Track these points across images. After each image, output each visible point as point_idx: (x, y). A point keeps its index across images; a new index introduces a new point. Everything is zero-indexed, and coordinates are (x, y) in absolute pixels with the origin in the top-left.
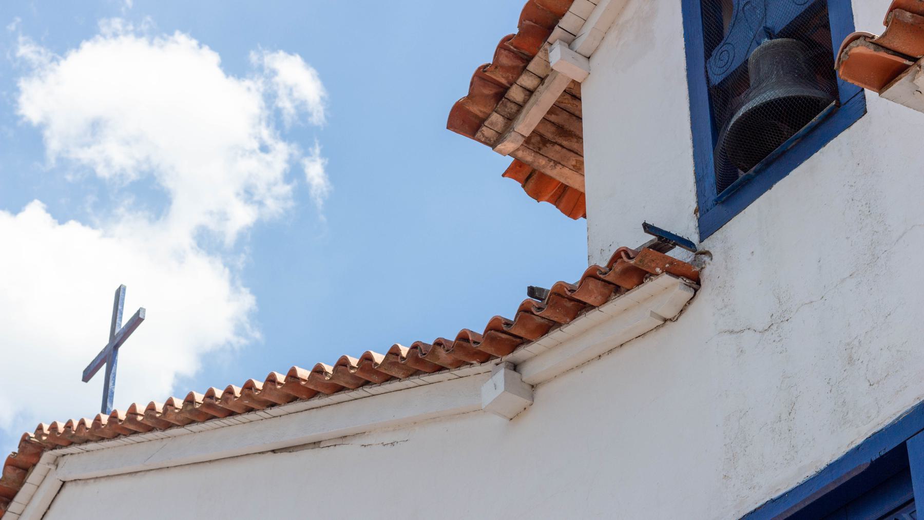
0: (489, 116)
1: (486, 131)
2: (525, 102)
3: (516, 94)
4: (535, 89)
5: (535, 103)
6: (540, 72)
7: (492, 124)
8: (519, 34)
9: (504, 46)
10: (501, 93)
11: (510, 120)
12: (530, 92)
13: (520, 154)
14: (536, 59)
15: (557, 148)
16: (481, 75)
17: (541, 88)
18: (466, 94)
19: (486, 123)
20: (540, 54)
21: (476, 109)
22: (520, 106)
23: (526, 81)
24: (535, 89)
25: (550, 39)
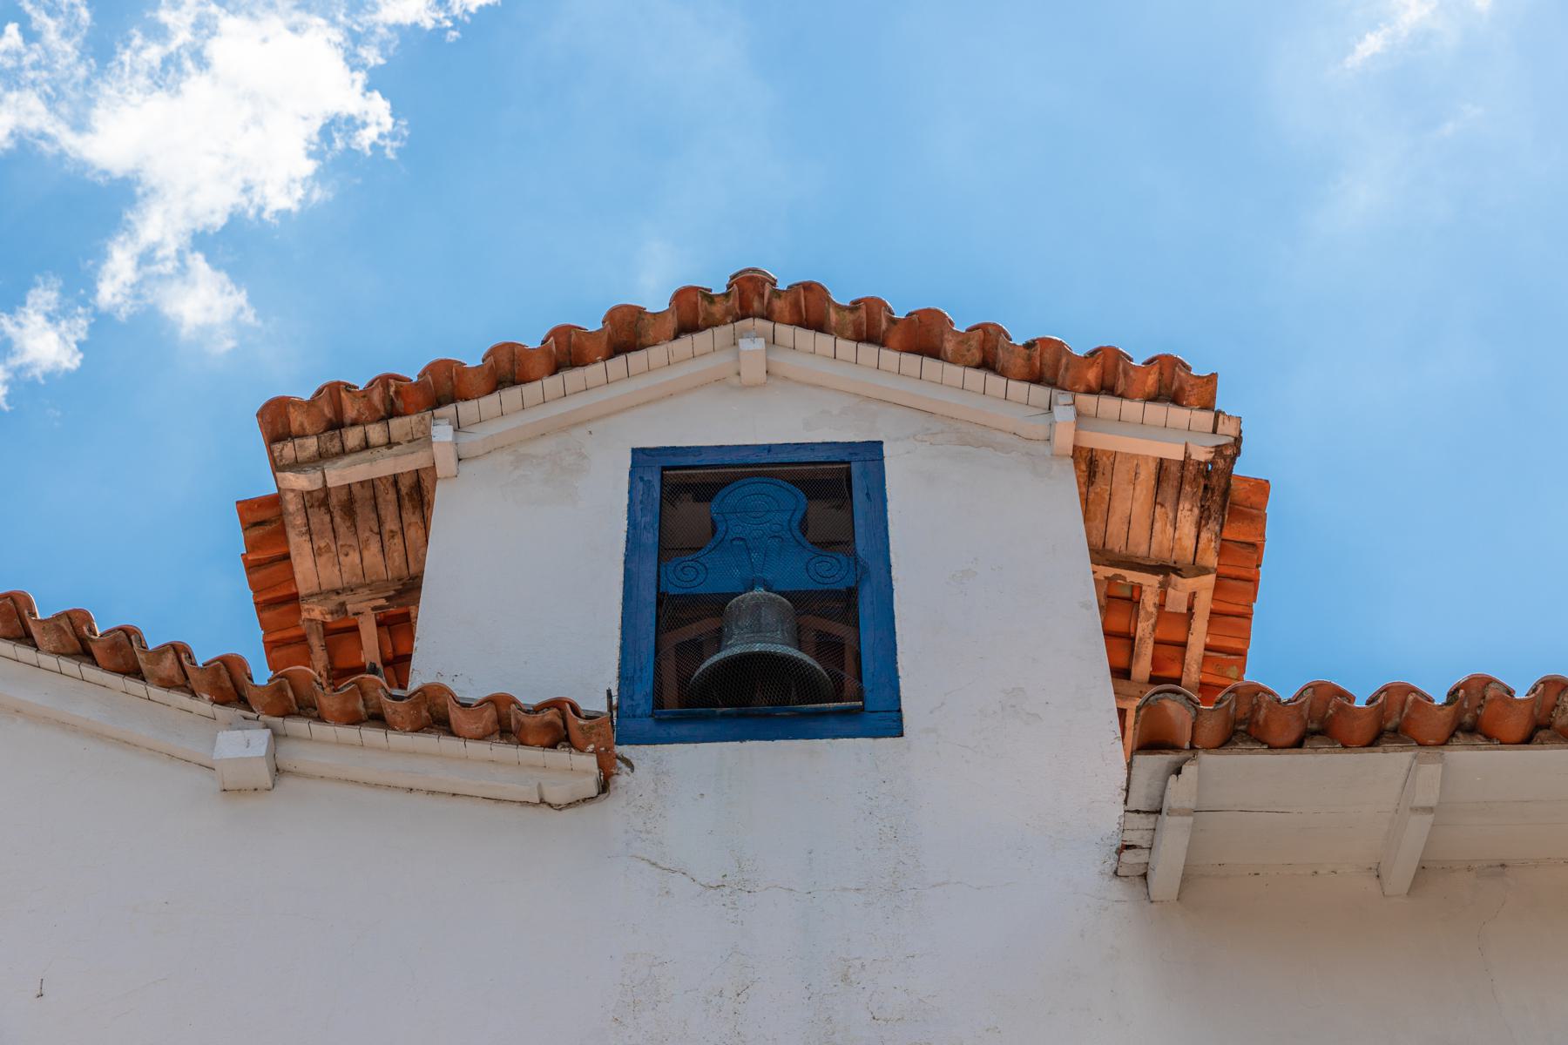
0: (304, 436)
1: (288, 450)
2: (353, 451)
3: (353, 437)
4: (374, 447)
5: (371, 461)
6: (395, 436)
7: (301, 446)
8: (417, 384)
9: (385, 380)
10: (337, 424)
11: (322, 457)
12: (366, 446)
13: (289, 496)
14: (406, 419)
15: (327, 518)
16: (335, 391)
17: (384, 450)
18: (307, 397)
19: (297, 441)
20: (414, 418)
21: (297, 419)
22: (344, 452)
23: (376, 433)
24: (374, 447)
25: (437, 412)
